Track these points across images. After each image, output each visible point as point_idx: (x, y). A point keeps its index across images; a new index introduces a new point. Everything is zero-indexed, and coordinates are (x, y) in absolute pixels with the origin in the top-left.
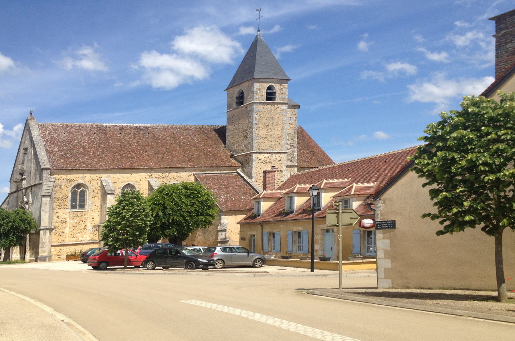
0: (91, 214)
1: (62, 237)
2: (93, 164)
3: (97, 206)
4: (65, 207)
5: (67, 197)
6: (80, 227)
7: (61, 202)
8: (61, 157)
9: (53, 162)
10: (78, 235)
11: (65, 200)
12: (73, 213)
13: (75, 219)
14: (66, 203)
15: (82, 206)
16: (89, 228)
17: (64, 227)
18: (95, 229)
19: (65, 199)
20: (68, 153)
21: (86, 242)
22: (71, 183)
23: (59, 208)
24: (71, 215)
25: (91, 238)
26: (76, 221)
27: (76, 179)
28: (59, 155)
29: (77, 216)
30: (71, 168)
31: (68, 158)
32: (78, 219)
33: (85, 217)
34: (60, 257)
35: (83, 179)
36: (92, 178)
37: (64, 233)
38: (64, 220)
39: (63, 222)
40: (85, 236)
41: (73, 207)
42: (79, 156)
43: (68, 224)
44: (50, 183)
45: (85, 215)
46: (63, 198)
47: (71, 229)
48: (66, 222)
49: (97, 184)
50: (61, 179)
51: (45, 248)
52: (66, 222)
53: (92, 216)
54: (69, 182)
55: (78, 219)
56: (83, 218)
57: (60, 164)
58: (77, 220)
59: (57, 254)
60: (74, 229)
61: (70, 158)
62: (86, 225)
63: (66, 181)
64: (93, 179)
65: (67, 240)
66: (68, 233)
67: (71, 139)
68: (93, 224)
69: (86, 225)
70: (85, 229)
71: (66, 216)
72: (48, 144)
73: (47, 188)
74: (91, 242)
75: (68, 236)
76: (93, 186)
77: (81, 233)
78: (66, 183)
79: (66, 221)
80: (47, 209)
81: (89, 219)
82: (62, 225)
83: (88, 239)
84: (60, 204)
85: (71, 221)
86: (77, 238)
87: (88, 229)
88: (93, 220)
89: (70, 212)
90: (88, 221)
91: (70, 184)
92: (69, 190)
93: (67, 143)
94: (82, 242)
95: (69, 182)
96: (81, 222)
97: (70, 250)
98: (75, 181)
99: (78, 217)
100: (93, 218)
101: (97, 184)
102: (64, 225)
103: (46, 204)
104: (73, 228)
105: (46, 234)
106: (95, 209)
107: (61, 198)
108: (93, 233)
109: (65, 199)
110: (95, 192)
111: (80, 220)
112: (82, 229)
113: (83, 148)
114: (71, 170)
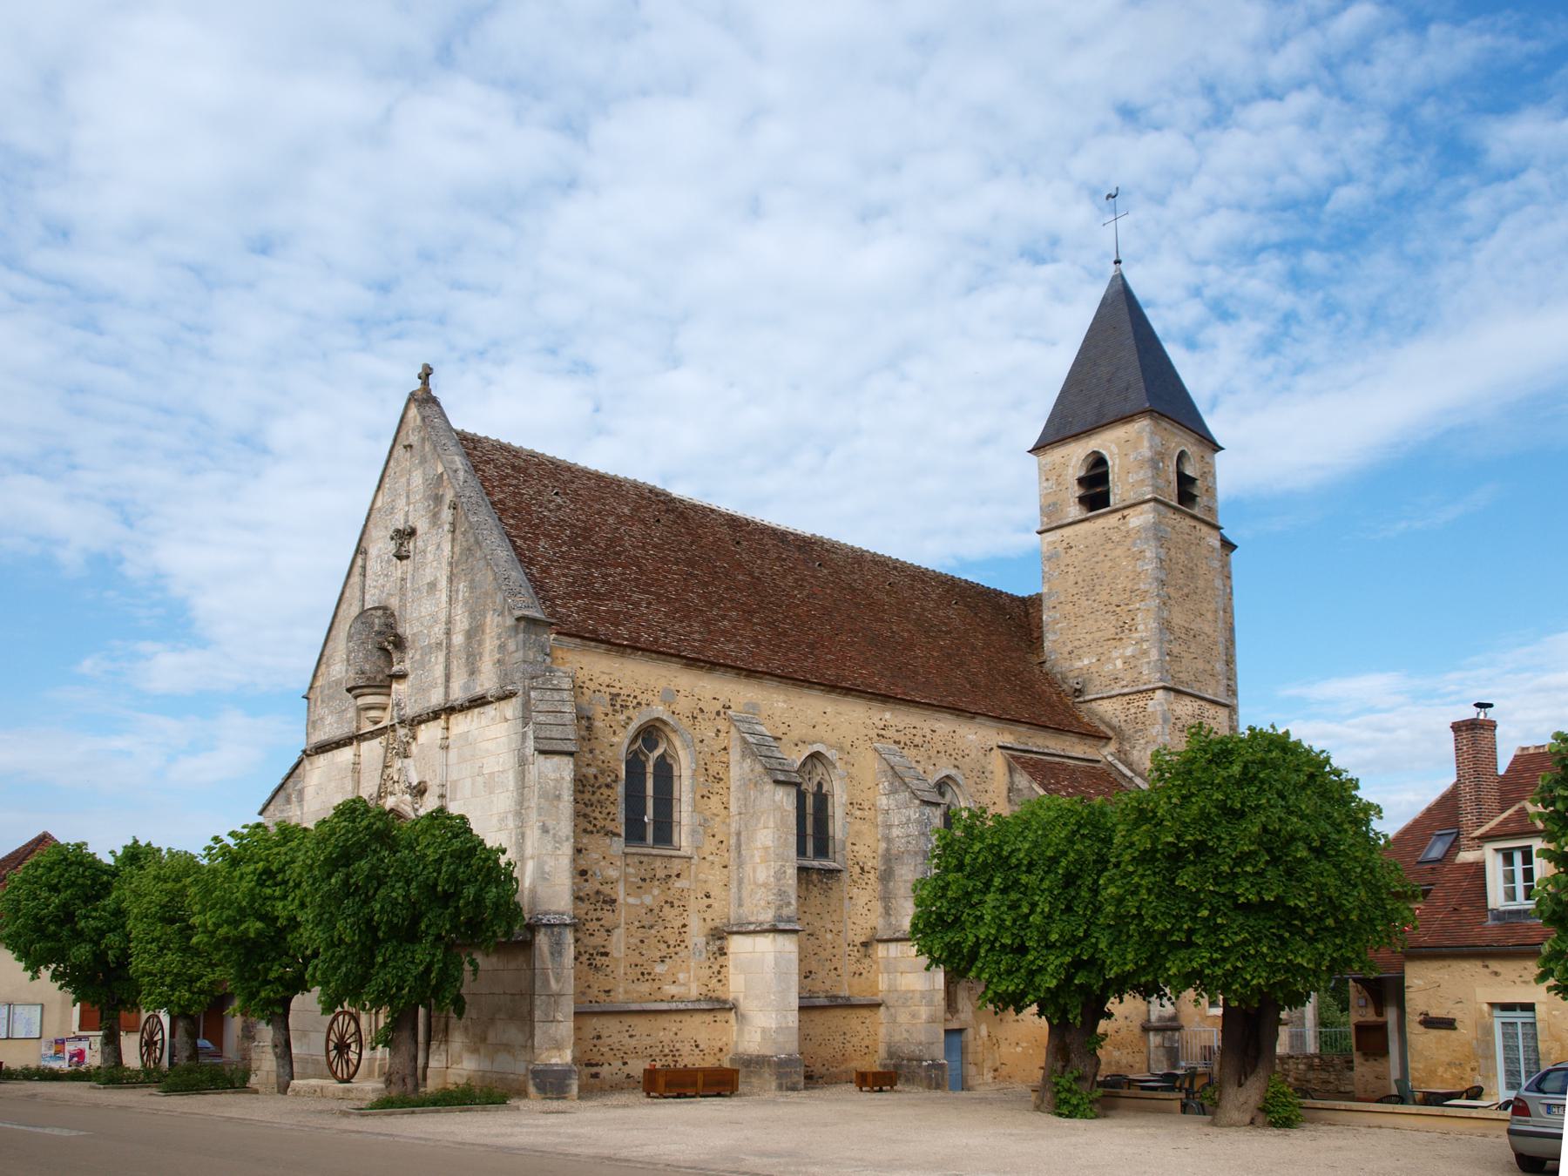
0: (702, 876)
1: (600, 975)
2: (695, 640)
3: (719, 838)
4: (610, 826)
5: (613, 776)
6: (663, 932)
7: (594, 799)
8: (572, 585)
9: (552, 600)
10: (659, 969)
11: (604, 790)
12: (636, 859)
13: (645, 893)
14: (612, 809)
15: (664, 832)
16: (696, 940)
17: (607, 925)
18: (715, 949)
19: (608, 786)
20: (591, 574)
21: (690, 1006)
22: (627, 713)
23: (585, 831)
24: (631, 870)
25: (704, 990)
26: (648, 900)
27: (642, 698)
28: (564, 575)
29: (652, 879)
30: (627, 639)
31: (599, 597)
32: (656, 892)
33: (679, 884)
34: (596, 1076)
35: (669, 697)
36: (701, 705)
37: (606, 954)
38: (606, 889)
39: (605, 902)
40: (682, 977)
41: (635, 833)
42: (635, 597)
43: (622, 916)
44: (557, 698)
45: (678, 876)
46: (601, 780)
47: (632, 940)
48: (614, 901)
49: (717, 735)
50: (593, 686)
51: (561, 1026)
52: (614, 901)
53: (705, 882)
54: (618, 707)
55: (656, 892)
56: (672, 892)
57: (577, 613)
58: (654, 896)
59: (585, 1059)
60: (642, 942)
61: (608, 596)
62: (684, 926)
63: (608, 697)
64: (702, 710)
65: (621, 990)
66: (622, 955)
67: (583, 522)
68: (710, 924)
69: (684, 926)
70: (683, 945)
71: (612, 873)
72: (512, 522)
73: (550, 719)
74: (704, 1006)
75: (622, 972)
76: (702, 741)
77: (667, 960)
78: (609, 710)
79: (614, 897)
80: (562, 823)
81: (692, 897)
82: (599, 914)
83: (694, 991)
84: (588, 810)
85: (631, 900)
86: (655, 986)
87: (691, 947)
88: (709, 901)
89: (626, 854)
90: (693, 905)
91: (621, 717)
92: (619, 744)
93: (578, 536)
94: (673, 1006)
95: (618, 707)
96: (667, 908)
97: (633, 1042)
98: (639, 704)
99: (657, 883)
100: (708, 897)
101: (717, 735)
102: (608, 918)
103: (558, 797)
104: (640, 934)
105: (560, 954)
106: (716, 851)
107: (592, 781)
108: (708, 963)
109: (608, 786)
110: (710, 772)
111: (662, 898)
112: (672, 943)
113: (639, 567)
114: (629, 651)
